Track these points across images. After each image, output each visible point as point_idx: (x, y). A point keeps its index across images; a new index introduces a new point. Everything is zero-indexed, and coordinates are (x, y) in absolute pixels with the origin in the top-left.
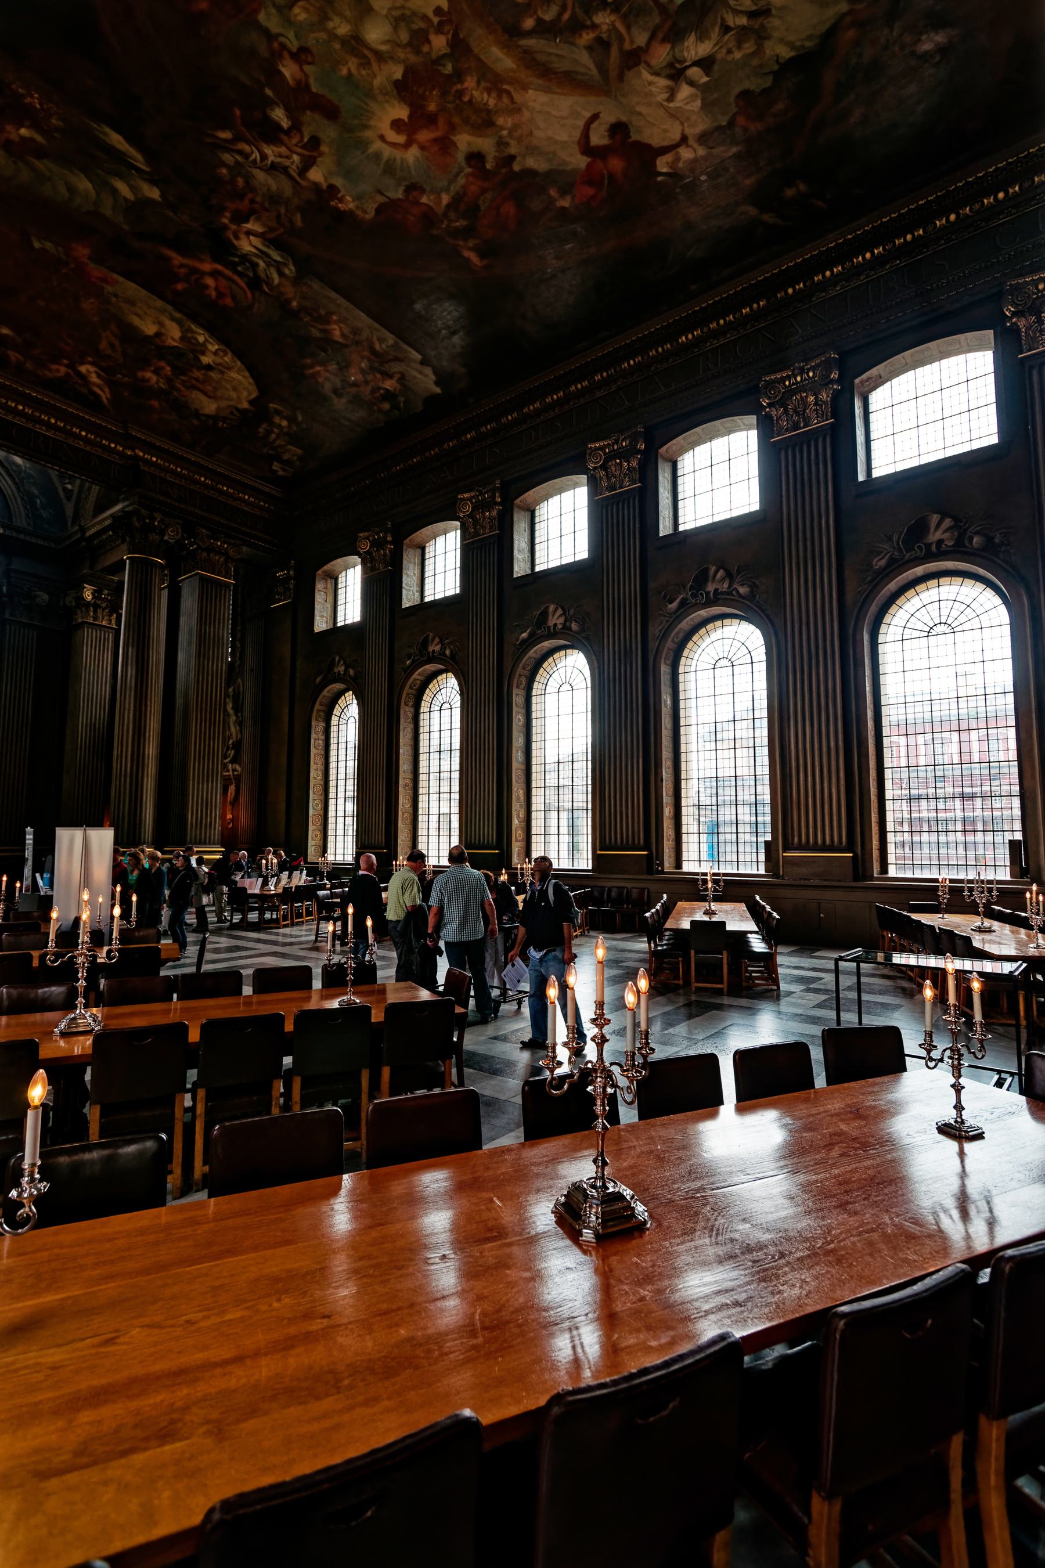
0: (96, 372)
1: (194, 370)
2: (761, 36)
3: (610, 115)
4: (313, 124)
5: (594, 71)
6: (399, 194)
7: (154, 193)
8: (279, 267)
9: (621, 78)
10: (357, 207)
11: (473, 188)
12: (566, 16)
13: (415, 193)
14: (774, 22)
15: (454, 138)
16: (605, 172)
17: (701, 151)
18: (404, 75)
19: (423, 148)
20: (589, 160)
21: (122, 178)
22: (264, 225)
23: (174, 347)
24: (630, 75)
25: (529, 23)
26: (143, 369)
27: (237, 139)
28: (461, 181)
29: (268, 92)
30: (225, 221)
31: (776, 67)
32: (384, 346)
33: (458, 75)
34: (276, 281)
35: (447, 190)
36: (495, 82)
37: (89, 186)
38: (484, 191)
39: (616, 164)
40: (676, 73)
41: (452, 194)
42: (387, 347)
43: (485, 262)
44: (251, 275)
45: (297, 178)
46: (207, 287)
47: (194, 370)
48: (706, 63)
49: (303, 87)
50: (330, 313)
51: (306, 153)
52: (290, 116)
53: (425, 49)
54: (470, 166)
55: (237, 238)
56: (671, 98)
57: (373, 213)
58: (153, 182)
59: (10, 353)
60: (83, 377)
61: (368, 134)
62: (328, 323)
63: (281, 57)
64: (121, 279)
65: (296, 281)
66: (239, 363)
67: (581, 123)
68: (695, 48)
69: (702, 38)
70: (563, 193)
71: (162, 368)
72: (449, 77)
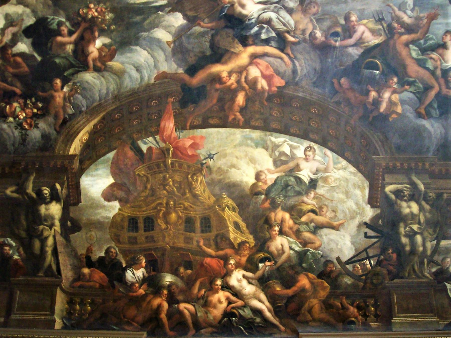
0: (244, 276)
1: (305, 199)
23: (276, 181)
26: (271, 238)
32: (409, 12)
34: (292, 23)
37: (145, 52)
42: (412, 10)
44: (274, 34)
47: (305, 199)
50: (347, 18)
58: (173, 10)
59: (183, 306)
60: (237, 294)
64: (204, 131)
66: (329, 152)
71: (283, 221)
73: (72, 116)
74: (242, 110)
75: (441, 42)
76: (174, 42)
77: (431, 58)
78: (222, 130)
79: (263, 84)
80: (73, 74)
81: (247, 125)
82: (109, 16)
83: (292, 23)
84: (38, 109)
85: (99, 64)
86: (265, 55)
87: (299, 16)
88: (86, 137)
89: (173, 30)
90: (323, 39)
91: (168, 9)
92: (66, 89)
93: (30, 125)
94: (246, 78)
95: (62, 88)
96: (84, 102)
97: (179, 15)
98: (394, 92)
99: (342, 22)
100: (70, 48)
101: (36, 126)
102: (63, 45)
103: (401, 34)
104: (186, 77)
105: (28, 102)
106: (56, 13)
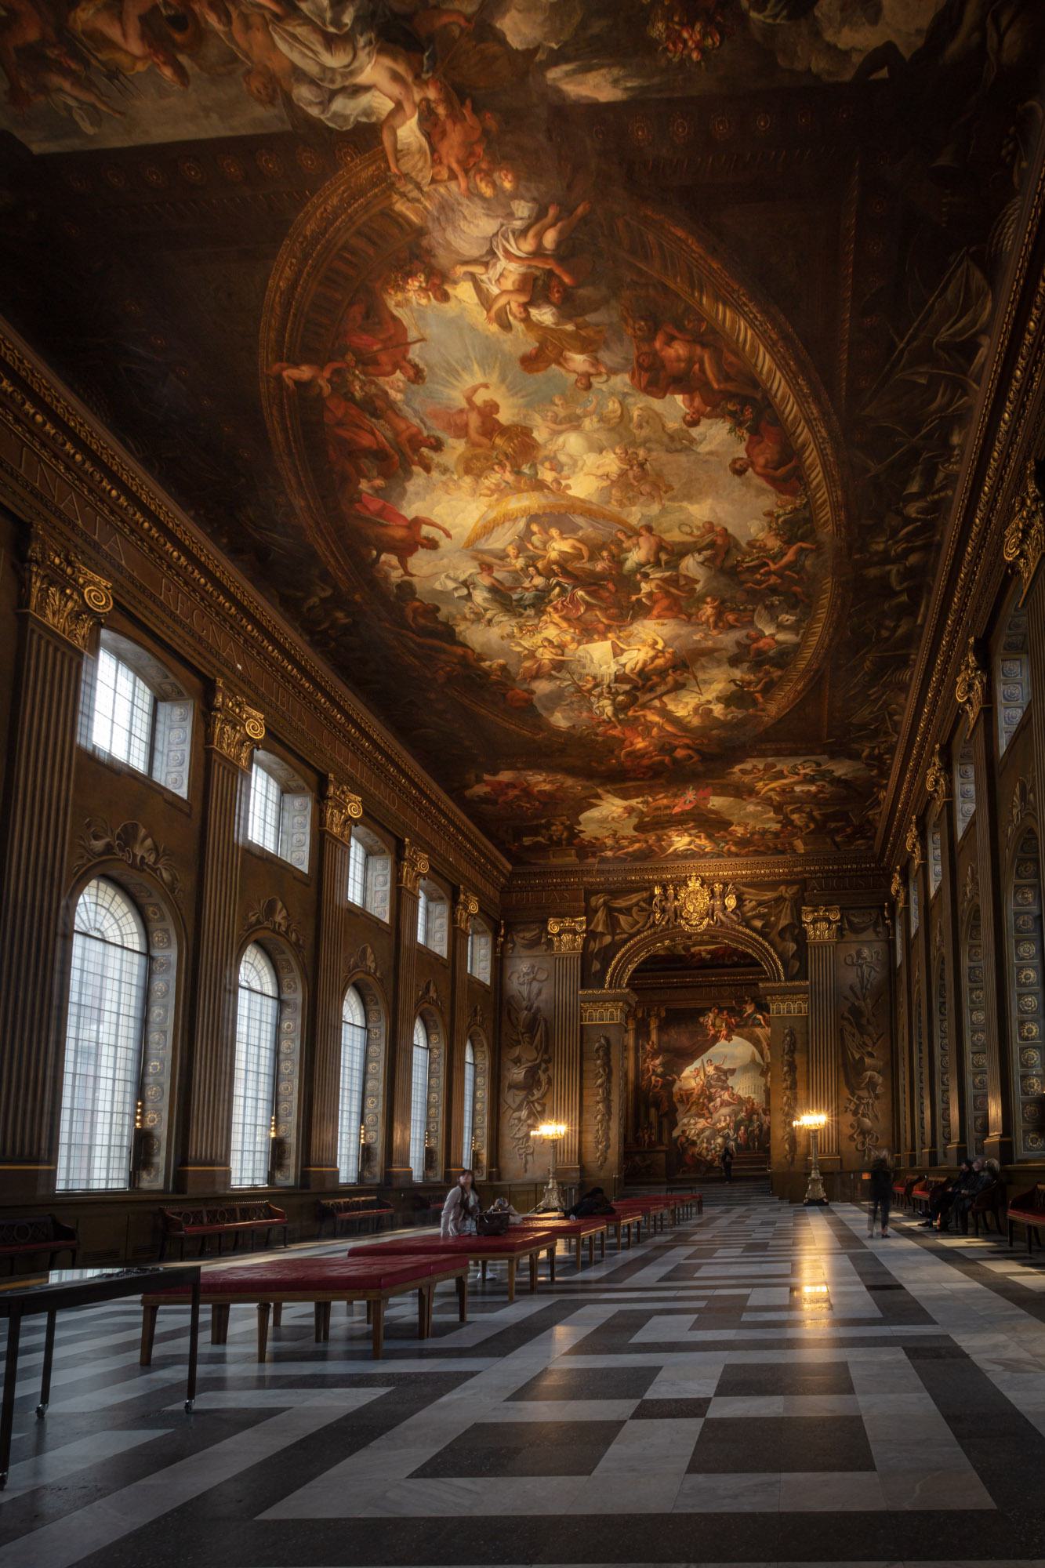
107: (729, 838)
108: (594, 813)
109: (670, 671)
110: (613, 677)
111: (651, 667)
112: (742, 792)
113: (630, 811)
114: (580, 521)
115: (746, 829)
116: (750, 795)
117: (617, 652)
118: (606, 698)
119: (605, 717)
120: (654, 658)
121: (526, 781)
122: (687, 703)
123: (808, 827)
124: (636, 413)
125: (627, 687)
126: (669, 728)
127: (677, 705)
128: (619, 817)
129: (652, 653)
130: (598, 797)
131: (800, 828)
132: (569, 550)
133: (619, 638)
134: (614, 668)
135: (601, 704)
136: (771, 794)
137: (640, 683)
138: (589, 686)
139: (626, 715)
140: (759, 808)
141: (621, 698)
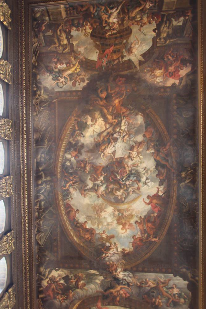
2: (148, 170)
3: (145, 197)
4: (113, 241)
5: (136, 195)
6: (133, 240)
7: (102, 278)
8: (128, 276)
9: (140, 192)
10: (129, 249)
11: (141, 227)
12: (126, 194)
13: (134, 237)
14: (148, 167)
15: (131, 223)
16: (155, 204)
17: (162, 187)
18: (117, 221)
19: (128, 229)
20: (150, 205)
21: (96, 279)
22: (121, 268)
24: (141, 190)
25: (123, 199)
27: (106, 254)
28: (138, 228)
29: (104, 242)
30: (114, 273)
31: (156, 169)
33: (123, 214)
34: (131, 281)
35: (138, 232)
36: (127, 210)
38: (143, 226)
39: (154, 201)
40: (146, 184)
41: (139, 231)
43: (158, 238)
44: (126, 283)
45: (117, 253)
46: (122, 294)
48: (147, 179)
49: (107, 237)
50: (146, 280)
51: (115, 247)
52: (109, 243)
53: (116, 215)
54: (137, 224)
55: (118, 275)
56: (149, 186)
57: (132, 248)
58: (101, 275)
61: (120, 235)
62: (148, 283)
63: (102, 235)
65: (134, 276)
67: (143, 202)
68: (143, 179)
69: (143, 178)
70: (153, 213)
72: (122, 215)
73: (74, 300)
74: (119, 301)
75: (172, 287)
76: (101, 283)
77: (170, 291)
78: (113, 306)
79: (124, 295)
80: (74, 290)
81: (120, 305)
82: (84, 276)
83: (131, 281)
84: (65, 297)
85: (81, 287)
86: (124, 288)
87: (133, 279)
88: (78, 306)
89: (100, 280)
90: (139, 285)
91: (99, 275)
92: (73, 293)
93: (63, 301)
94: (119, 293)
95: (72, 292)
96: (77, 297)
97: (102, 277)
98: (160, 299)
99: (144, 281)
100: (74, 283)
101: (64, 302)
102: (72, 282)
103: (161, 284)
104: (104, 292)
105: (63, 295)
106: (71, 274)
107: (93, 21)
108: (146, 48)
109: (101, 142)
110: (118, 141)
111: (106, 145)
112: (86, 65)
113: (130, 51)
114: (113, 200)
115: (85, 30)
116: (82, 61)
117: (114, 153)
118: (122, 130)
119: (125, 119)
120: (105, 149)
121: (163, 78)
122: (98, 126)
123: (60, 30)
124: (96, 225)
125: (115, 135)
126: (105, 111)
127: (102, 124)
128: (135, 44)
129: (105, 151)
130: (140, 63)
131: (63, 30)
132: (118, 192)
133: (113, 159)
134: (116, 146)
135: (125, 127)
136: (74, 62)
137: (110, 137)
138: (126, 137)
139: (118, 120)
140: (79, 49)
141: (118, 130)
